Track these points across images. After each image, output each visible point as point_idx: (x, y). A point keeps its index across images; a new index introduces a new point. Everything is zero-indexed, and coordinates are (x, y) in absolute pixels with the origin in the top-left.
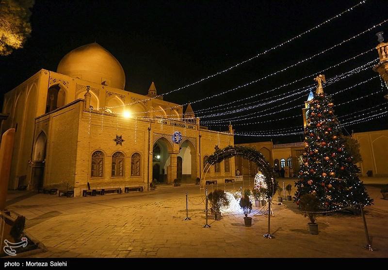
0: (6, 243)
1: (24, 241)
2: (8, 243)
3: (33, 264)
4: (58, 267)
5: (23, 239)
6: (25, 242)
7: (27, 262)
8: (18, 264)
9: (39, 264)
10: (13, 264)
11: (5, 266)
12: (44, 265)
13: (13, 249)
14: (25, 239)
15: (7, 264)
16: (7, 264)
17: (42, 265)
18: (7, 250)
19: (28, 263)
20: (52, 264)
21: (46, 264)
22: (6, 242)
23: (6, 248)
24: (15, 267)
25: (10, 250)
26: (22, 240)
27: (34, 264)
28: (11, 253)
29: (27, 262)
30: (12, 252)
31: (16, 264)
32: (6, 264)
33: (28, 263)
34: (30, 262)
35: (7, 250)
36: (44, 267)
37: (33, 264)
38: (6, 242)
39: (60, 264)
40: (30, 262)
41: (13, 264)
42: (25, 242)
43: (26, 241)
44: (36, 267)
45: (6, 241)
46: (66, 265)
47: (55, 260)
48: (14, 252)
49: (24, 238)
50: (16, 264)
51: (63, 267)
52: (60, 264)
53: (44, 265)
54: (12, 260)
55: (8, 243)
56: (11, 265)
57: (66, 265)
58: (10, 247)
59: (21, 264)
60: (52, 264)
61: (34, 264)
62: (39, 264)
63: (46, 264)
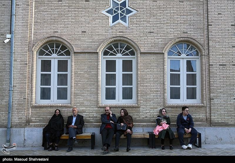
1: (15, 145)
6: (15, 146)
7: (15, 158)
10: (8, 160)
11: (3, 160)
14: (15, 145)
15: (4, 160)
16: (4, 160)
22: (3, 146)
23: (3, 150)
24: (9, 161)
25: (6, 151)
26: (13, 145)
29: (15, 158)
30: (7, 152)
32: (4, 160)
35: (4, 151)
41: (8, 160)
42: (15, 146)
48: (8, 152)
56: (7, 160)
58: (6, 149)
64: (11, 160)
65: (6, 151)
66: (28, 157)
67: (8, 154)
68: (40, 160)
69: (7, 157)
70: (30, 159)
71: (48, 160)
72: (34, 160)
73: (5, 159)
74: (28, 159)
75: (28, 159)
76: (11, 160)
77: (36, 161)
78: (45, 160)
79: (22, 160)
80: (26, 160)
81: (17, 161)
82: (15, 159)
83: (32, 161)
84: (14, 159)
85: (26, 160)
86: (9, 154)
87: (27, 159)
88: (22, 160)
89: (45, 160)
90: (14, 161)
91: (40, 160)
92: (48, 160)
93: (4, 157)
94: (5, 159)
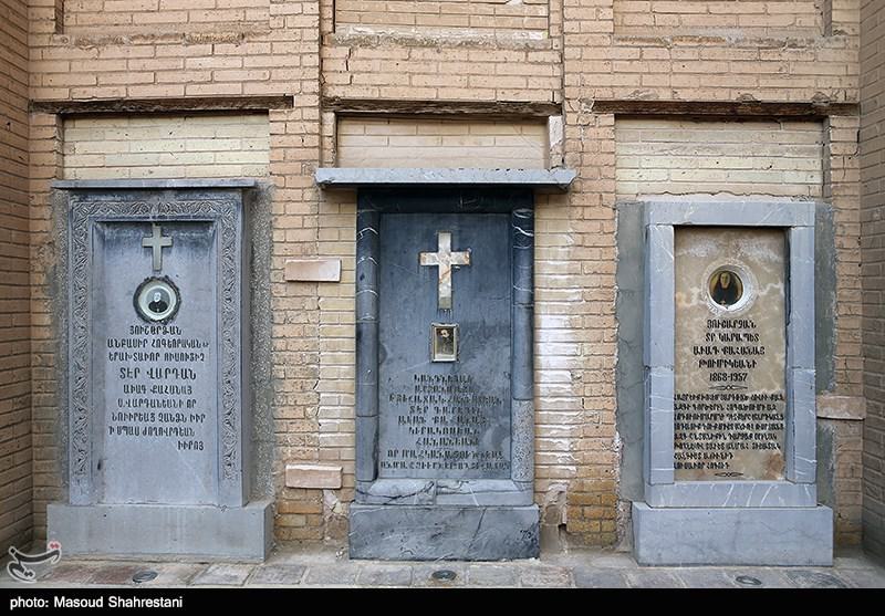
0: (13, 555)
1: (55, 549)
2: (17, 555)
5: (52, 546)
6: (56, 553)
7: (56, 598)
10: (29, 603)
11: (12, 606)
13: (28, 567)
14: (57, 546)
15: (15, 603)
22: (13, 551)
23: (13, 566)
24: (34, 610)
25: (22, 570)
26: (49, 546)
28: (24, 577)
29: (56, 598)
32: (14, 603)
35: (15, 571)
38: (13, 551)
41: (29, 603)
42: (56, 553)
48: (31, 574)
55: (17, 555)
56: (26, 604)
58: (17, 562)
64: (41, 603)
65: (22, 570)
66: (106, 593)
68: (149, 603)
69: (27, 593)
70: (114, 602)
71: (180, 604)
72: (129, 603)
73: (20, 600)
74: (106, 602)
75: (106, 602)
76: (41, 603)
77: (135, 610)
78: (169, 603)
79: (84, 603)
80: (98, 603)
81: (64, 610)
82: (58, 602)
83: (121, 610)
84: (52, 602)
85: (98, 603)
87: (101, 600)
88: (84, 603)
89: (169, 603)
90: (51, 609)
91: (149, 603)
92: (180, 604)
93: (16, 593)
94: (20, 600)
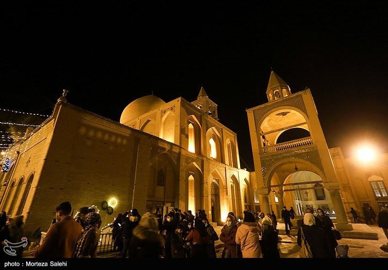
0: (6, 243)
1: (25, 241)
2: (8, 243)
3: (33, 264)
4: (58, 267)
5: (23, 239)
6: (25, 242)
7: (27, 262)
8: (18, 264)
9: (39, 264)
10: (13, 264)
11: (5, 266)
12: (44, 265)
14: (25, 239)
15: (7, 264)
16: (7, 264)
17: (42, 265)
18: (7, 250)
19: (28, 263)
20: (53, 264)
21: (46, 264)
23: (6, 248)
25: (10, 250)
26: (22, 239)
27: (34, 264)
29: (27, 262)
30: (12, 252)
31: (16, 264)
32: (6, 264)
33: (28, 263)
34: (30, 262)
35: (7, 250)
36: (44, 267)
37: (33, 264)
38: (6, 242)
39: (60, 264)
40: (30, 262)
41: (13, 264)
42: (25, 242)
43: (26, 241)
44: (36, 267)
45: (6, 242)
46: (66, 265)
47: (55, 261)
48: (14, 252)
49: (24, 238)
50: (16, 264)
51: (63, 267)
52: (60, 264)
53: (44, 265)
54: (12, 259)
55: (8, 243)
56: (11, 265)
57: (66, 265)
58: (10, 247)
59: (21, 264)
60: (53, 264)
61: (34, 264)
62: (39, 264)
63: (46, 264)
65: (10, 250)
67: (14, 254)
86: (16, 255)
